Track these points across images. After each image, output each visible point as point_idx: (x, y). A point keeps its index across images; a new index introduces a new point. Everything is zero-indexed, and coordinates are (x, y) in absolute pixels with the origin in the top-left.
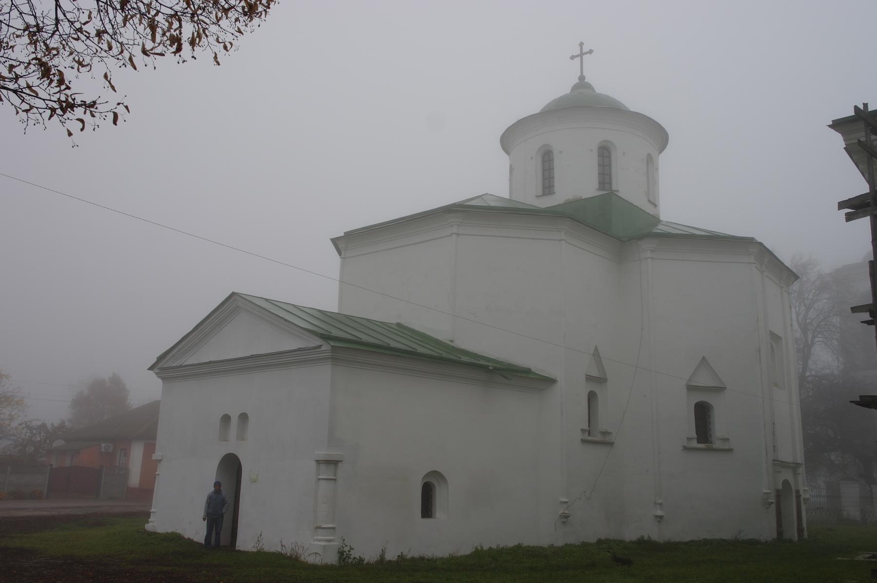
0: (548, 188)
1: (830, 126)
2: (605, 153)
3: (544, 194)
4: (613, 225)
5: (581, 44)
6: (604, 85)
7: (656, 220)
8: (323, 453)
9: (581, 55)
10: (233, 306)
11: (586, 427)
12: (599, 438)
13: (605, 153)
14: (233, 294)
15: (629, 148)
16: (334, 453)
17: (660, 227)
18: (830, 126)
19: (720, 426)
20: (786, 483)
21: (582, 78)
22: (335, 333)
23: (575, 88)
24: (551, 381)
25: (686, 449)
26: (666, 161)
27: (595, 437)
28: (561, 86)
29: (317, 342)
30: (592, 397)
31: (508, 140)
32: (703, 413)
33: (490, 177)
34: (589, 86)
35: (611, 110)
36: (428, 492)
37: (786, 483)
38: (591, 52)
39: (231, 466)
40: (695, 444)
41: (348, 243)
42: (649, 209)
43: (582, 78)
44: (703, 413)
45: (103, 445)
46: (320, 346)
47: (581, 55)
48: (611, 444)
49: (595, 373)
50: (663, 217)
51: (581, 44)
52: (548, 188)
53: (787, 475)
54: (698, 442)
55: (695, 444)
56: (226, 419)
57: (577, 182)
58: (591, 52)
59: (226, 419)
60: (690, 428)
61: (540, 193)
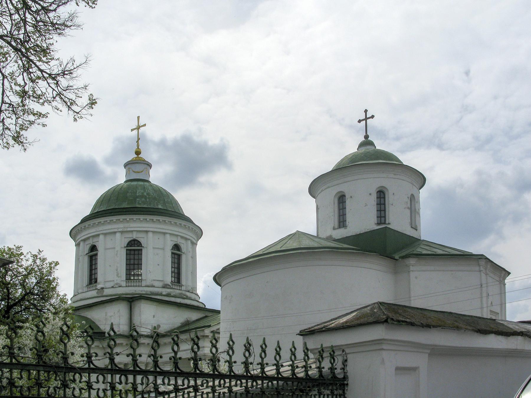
0: (342, 223)
2: (381, 194)
3: (340, 227)
5: (366, 111)
9: (366, 119)
13: (381, 194)
21: (366, 137)
23: (362, 145)
31: (314, 188)
33: (304, 218)
34: (371, 144)
38: (373, 117)
43: (366, 137)
47: (366, 119)
51: (366, 111)
52: (342, 223)
58: (373, 117)
61: (336, 226)
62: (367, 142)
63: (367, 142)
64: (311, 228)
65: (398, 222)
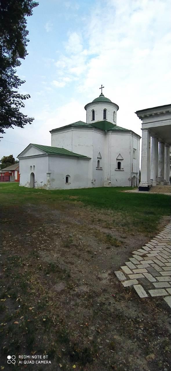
1: (135, 113)
2: (105, 111)
4: (105, 127)
5: (102, 85)
6: (106, 96)
7: (115, 125)
8: (47, 172)
9: (102, 88)
10: (31, 146)
11: (97, 167)
12: (100, 169)
13: (105, 111)
14: (30, 144)
15: (110, 109)
16: (50, 172)
17: (115, 127)
18: (135, 113)
19: (122, 166)
20: (134, 176)
21: (102, 93)
22: (50, 151)
23: (100, 96)
24: (91, 159)
25: (115, 170)
26: (118, 112)
27: (99, 168)
28: (97, 96)
29: (45, 153)
30: (98, 161)
31: (86, 108)
32: (119, 164)
33: (82, 117)
35: (108, 102)
36: (67, 178)
37: (134, 176)
39: (33, 174)
40: (117, 170)
41: (53, 132)
42: (114, 123)
43: (102, 93)
44: (119, 164)
45: (9, 172)
46: (46, 154)
47: (102, 88)
48: (102, 170)
49: (99, 157)
50: (117, 125)
51: (102, 85)
52: (93, 119)
53: (135, 175)
54: (118, 169)
55: (117, 170)
56: (31, 166)
57: (99, 118)
58: (104, 87)
59: (31, 166)
60: (116, 166)
62: (102, 95)
63: (102, 95)
64: (84, 120)
65: (109, 119)
